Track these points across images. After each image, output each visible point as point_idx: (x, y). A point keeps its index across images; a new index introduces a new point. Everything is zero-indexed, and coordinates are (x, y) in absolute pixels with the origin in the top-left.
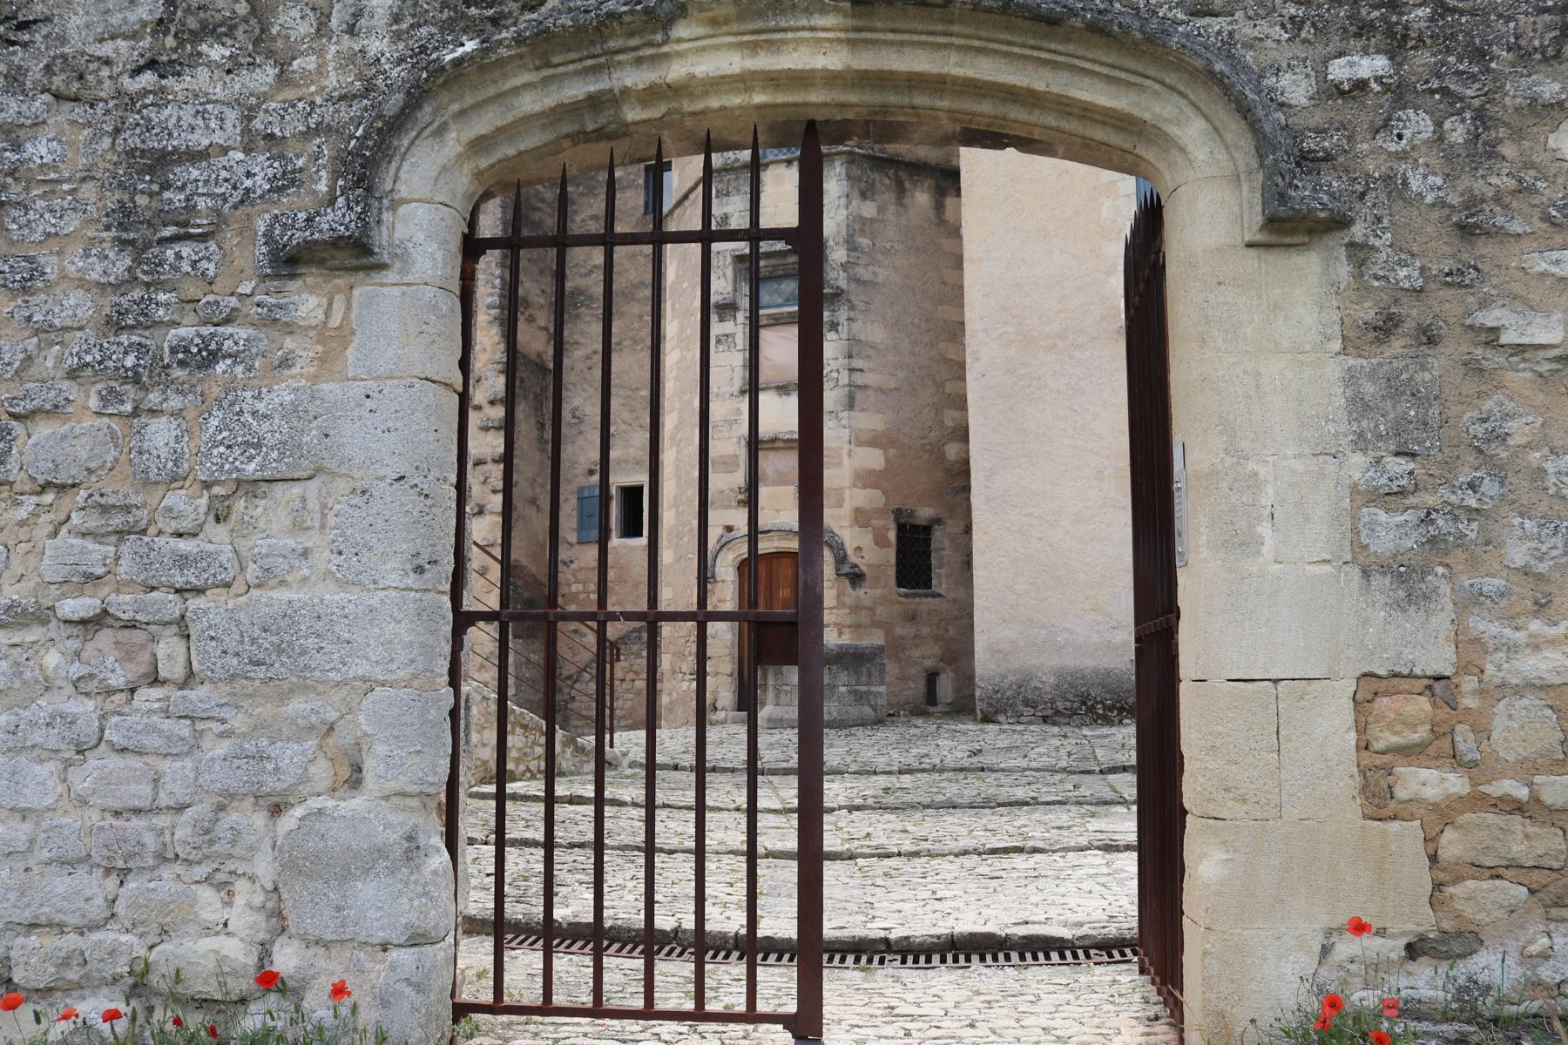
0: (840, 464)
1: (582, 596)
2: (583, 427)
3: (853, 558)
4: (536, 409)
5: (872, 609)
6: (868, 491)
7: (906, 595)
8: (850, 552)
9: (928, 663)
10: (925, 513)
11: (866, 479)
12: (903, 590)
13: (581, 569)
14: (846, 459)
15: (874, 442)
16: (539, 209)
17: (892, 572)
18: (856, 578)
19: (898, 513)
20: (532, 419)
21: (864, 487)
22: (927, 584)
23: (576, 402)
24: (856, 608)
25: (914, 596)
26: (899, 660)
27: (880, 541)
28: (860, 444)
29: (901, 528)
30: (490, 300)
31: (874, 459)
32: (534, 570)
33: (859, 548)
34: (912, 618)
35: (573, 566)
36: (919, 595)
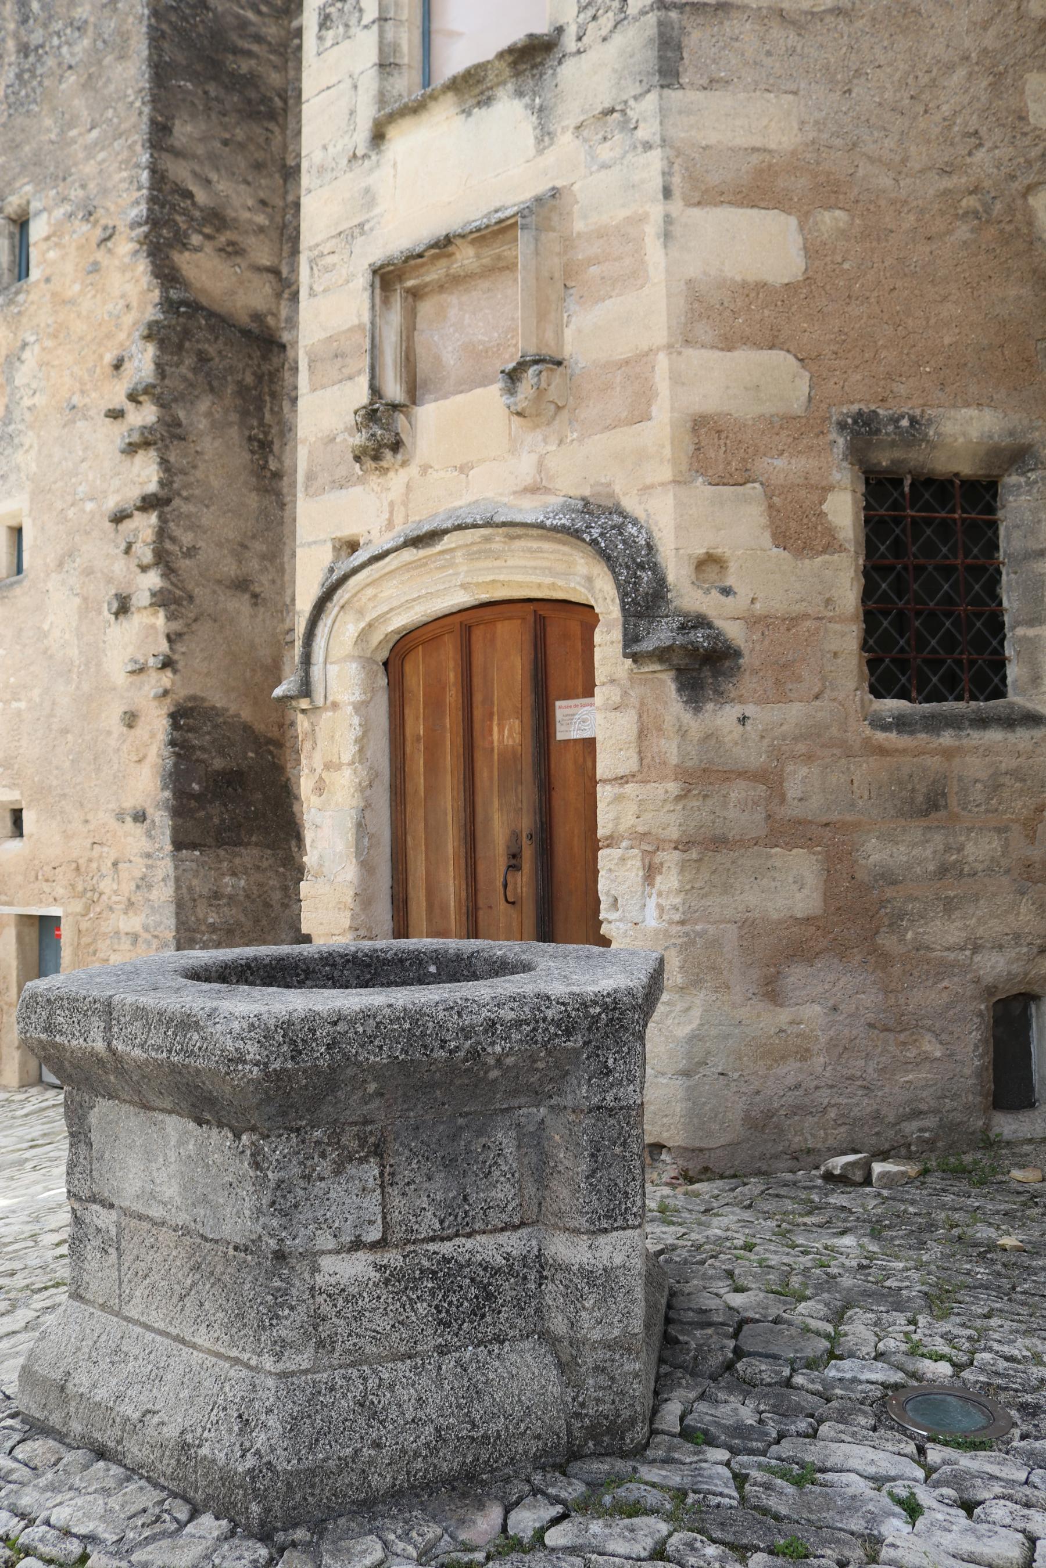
0: (636, 276)
3: (687, 595)
4: (245, 413)
5: (769, 779)
6: (745, 358)
7: (901, 724)
8: (676, 572)
9: (996, 966)
10: (963, 431)
11: (731, 315)
12: (892, 705)
14: (655, 254)
15: (759, 187)
16: (249, 54)
17: (846, 639)
18: (703, 665)
19: (862, 430)
20: (234, 432)
21: (728, 344)
22: (989, 681)
24: (701, 778)
25: (933, 724)
26: (883, 959)
27: (796, 529)
28: (707, 196)
29: (880, 489)
31: (766, 247)
32: (246, 714)
33: (709, 563)
34: (930, 803)
36: (955, 722)
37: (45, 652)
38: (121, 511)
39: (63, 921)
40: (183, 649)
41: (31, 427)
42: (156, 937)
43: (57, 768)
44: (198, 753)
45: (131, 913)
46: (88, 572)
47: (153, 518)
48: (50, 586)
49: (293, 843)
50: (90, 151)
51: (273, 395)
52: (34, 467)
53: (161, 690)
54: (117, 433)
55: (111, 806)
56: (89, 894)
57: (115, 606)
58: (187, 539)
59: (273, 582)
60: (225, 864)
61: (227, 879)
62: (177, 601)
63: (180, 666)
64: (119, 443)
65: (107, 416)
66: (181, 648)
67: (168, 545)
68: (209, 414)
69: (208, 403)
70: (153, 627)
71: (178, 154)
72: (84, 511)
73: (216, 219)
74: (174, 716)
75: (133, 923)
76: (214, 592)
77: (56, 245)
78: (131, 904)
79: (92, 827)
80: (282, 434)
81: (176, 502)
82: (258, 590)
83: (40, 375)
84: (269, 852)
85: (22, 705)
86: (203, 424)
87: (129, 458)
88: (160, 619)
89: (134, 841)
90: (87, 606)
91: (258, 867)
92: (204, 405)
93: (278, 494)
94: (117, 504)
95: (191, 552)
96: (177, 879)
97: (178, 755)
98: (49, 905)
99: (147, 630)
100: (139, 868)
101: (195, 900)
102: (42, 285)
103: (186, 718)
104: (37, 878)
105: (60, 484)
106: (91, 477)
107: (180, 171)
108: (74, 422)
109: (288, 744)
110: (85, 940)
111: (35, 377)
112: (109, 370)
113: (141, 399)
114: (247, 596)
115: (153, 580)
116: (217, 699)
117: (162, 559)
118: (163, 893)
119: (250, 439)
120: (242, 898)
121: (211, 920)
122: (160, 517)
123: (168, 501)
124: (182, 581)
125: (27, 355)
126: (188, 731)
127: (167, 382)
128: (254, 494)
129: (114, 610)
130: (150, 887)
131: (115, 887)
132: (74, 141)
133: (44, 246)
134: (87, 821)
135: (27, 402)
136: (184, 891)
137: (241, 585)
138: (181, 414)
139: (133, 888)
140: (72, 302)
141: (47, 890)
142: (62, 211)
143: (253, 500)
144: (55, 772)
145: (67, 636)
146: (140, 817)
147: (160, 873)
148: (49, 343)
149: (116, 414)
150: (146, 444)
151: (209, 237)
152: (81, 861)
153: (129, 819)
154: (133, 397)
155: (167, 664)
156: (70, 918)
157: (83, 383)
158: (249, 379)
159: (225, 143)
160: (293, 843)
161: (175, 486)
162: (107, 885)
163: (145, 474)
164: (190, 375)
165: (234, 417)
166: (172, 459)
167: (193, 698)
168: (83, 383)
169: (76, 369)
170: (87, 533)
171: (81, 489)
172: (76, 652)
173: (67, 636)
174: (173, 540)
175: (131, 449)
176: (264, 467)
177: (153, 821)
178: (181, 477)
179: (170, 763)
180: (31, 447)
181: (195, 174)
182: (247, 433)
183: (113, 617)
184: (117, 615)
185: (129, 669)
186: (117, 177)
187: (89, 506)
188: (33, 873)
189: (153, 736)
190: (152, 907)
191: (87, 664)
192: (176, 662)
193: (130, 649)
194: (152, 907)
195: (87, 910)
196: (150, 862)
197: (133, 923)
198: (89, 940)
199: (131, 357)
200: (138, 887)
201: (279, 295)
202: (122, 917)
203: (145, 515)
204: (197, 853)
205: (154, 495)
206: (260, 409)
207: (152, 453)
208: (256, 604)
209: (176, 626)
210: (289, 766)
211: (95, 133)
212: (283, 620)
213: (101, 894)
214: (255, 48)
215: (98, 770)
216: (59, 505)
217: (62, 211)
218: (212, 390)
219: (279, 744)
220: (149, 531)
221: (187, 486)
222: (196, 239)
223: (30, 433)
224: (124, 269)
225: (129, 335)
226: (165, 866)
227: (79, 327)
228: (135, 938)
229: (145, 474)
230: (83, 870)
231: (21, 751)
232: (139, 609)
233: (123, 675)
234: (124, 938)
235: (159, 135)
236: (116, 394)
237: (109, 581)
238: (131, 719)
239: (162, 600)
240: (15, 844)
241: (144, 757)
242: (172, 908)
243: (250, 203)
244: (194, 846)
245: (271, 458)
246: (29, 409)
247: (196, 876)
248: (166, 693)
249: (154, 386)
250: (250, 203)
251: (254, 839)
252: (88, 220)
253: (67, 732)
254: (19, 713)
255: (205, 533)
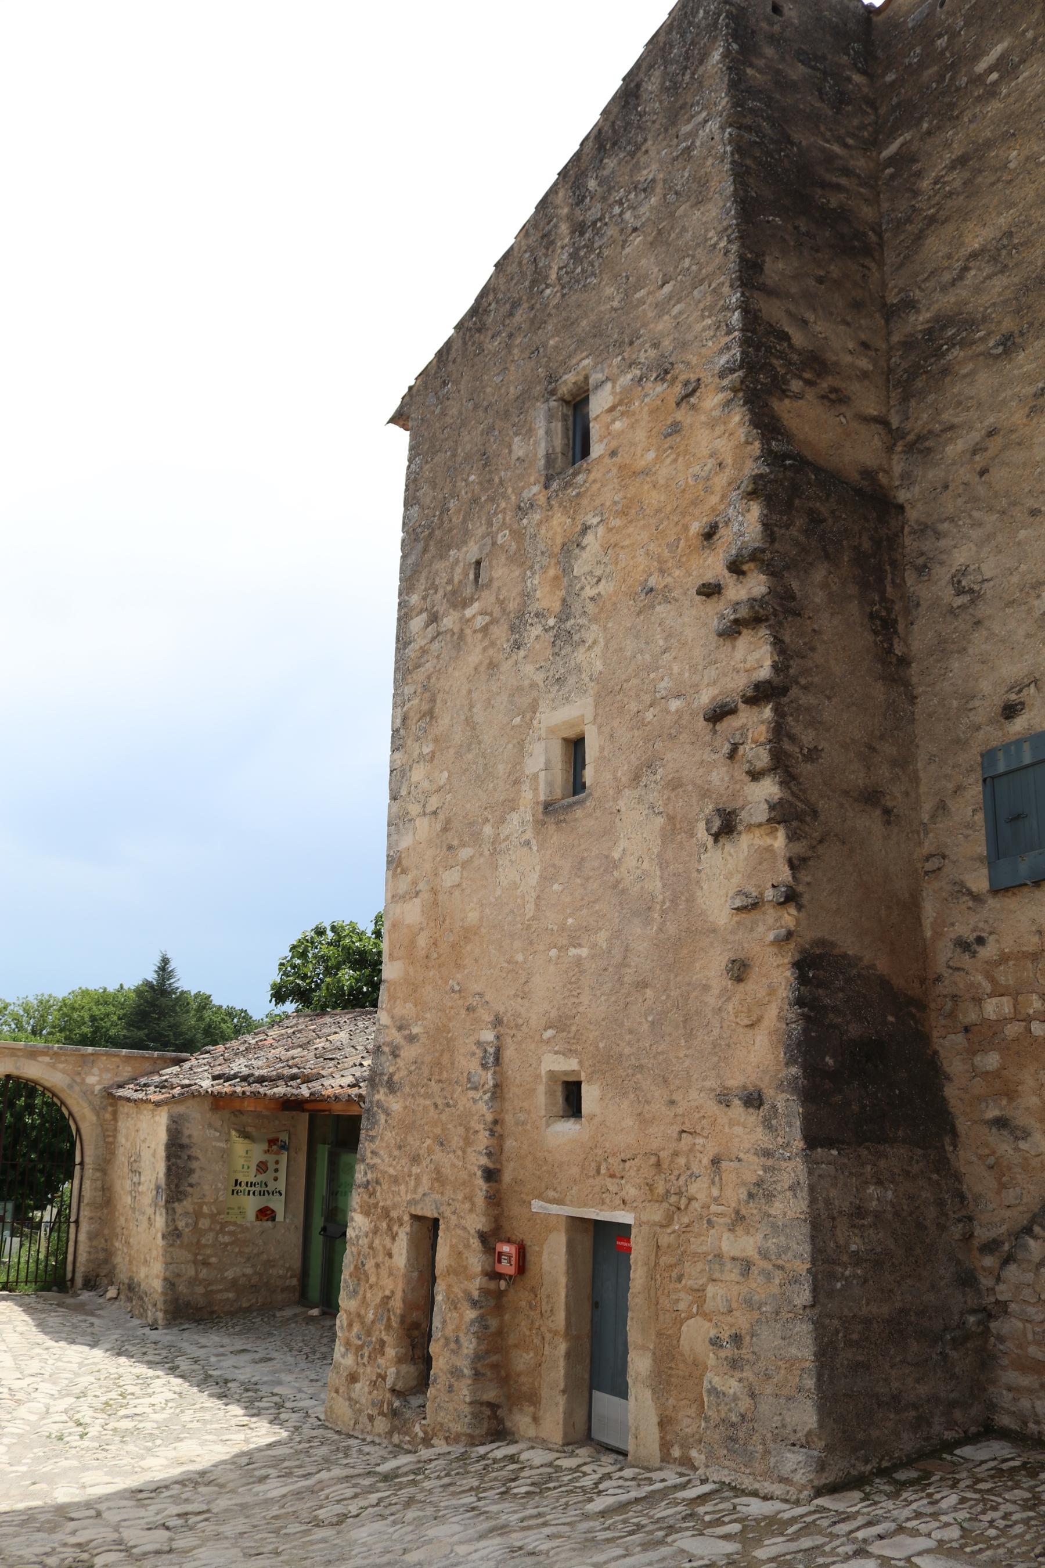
1: (1013, 1030)
2: (982, 610)
13: (1004, 958)
16: (838, 188)
20: (853, 607)
23: (960, 557)
30: (723, 360)
32: (883, 966)
35: (986, 952)
37: (615, 887)
38: (721, 706)
39: (634, 1231)
40: (808, 879)
41: (594, 619)
42: (780, 1268)
43: (631, 1032)
44: (831, 1015)
45: (739, 1230)
46: (675, 784)
47: (768, 712)
48: (621, 804)
49: (947, 1140)
50: (662, 308)
51: (893, 563)
52: (599, 666)
53: (783, 932)
54: (712, 615)
55: (708, 1084)
56: (673, 1199)
57: (717, 824)
58: (808, 737)
59: (907, 794)
60: (869, 1167)
61: (871, 1189)
62: (800, 817)
63: (805, 900)
64: (715, 624)
65: (699, 593)
66: (805, 877)
67: (787, 746)
68: (825, 585)
69: (824, 572)
70: (769, 849)
71: (771, 292)
72: (668, 712)
73: (816, 363)
74: (797, 965)
75: (746, 1244)
76: (841, 806)
77: (623, 414)
78: (739, 1218)
79: (680, 1111)
80: (907, 611)
81: (794, 691)
82: (890, 804)
83: (606, 560)
84: (920, 1152)
85: (584, 952)
86: (819, 597)
87: (728, 644)
88: (779, 841)
89: (745, 1132)
90: (675, 828)
91: (907, 1173)
92: (819, 574)
93: (907, 684)
94: (714, 698)
95: (812, 755)
96: (812, 1189)
97: (806, 1018)
98: (614, 1208)
99: (758, 855)
100: (753, 1169)
101: (834, 1219)
102: (607, 460)
103: (814, 967)
104: (598, 1172)
105: (634, 681)
106: (676, 669)
107: (774, 311)
108: (654, 607)
109: (933, 1006)
110: (664, 1260)
111: (599, 562)
112: (697, 542)
113: (745, 567)
114: (878, 812)
115: (769, 789)
116: (849, 945)
117: (781, 764)
118: (790, 1207)
119: (872, 616)
120: (890, 1216)
121: (854, 1247)
122: (776, 710)
123: (784, 691)
124: (804, 791)
125: (589, 539)
126: (818, 986)
127: (777, 545)
128: (879, 684)
129: (715, 829)
130: (770, 1197)
131: (715, 1192)
132: (642, 302)
133: (608, 418)
134: (672, 1102)
135: (589, 592)
136: (821, 1205)
137: (871, 797)
138: (795, 585)
139: (744, 1196)
140: (646, 472)
141: (613, 1188)
142: (629, 376)
143: (879, 691)
144: (628, 1037)
145: (646, 865)
146: (753, 1100)
147: (786, 1179)
148: (617, 522)
149: (710, 591)
150: (754, 621)
151: (809, 383)
152: (662, 1154)
153: (737, 1102)
154: (736, 568)
155: (791, 897)
156: (645, 1229)
157: (661, 561)
158: (867, 545)
159: (820, 280)
160: (947, 1140)
161: (792, 671)
162: (699, 1189)
163: (755, 657)
164: (802, 538)
165: (852, 590)
166: (787, 639)
167: (821, 942)
168: (661, 561)
169: (652, 546)
170: (672, 738)
171: (662, 685)
172: (659, 884)
173: (646, 865)
174: (792, 738)
175: (732, 631)
176: (890, 651)
177: (774, 1107)
178: (798, 661)
179: (797, 1028)
180: (595, 642)
181: (789, 313)
182: (868, 609)
183: (711, 839)
184: (716, 837)
185: (738, 903)
186: (699, 327)
187: (675, 705)
188: (593, 1165)
189: (772, 992)
190: (774, 1226)
191: (674, 901)
192: (801, 895)
193: (736, 879)
194: (774, 1226)
195: (669, 1220)
196: (770, 1162)
197: (746, 1244)
198: (672, 1260)
199: (727, 523)
200: (751, 1195)
201: (890, 449)
202: (726, 1235)
203: (755, 709)
204: (835, 1152)
205: (768, 682)
206: (881, 580)
207: (764, 631)
208: (888, 823)
209: (800, 848)
210: (935, 1034)
211: (667, 288)
212: (920, 844)
213: (690, 1200)
214: (843, 181)
215: (690, 1036)
216: (634, 707)
217: (629, 376)
218: (827, 557)
219: (922, 1006)
220: (763, 728)
221: (805, 672)
222: (796, 385)
223: (594, 627)
224: (712, 425)
225: (723, 497)
226: (793, 1170)
227: (655, 498)
228: (746, 1266)
229: (755, 657)
230: (665, 1166)
231: (581, 1009)
232: (750, 827)
233: (727, 910)
234: (729, 1265)
235: (750, 274)
236: (713, 566)
237: (705, 794)
238: (739, 970)
239: (782, 815)
240: (568, 1128)
241: (759, 1020)
242: (806, 1229)
243: (851, 345)
244: (829, 1143)
245: (896, 641)
246: (592, 599)
247: (834, 1185)
248: (790, 935)
249: (763, 551)
250: (851, 345)
251: (900, 1133)
252: (663, 380)
253: (646, 986)
254: (578, 961)
255: (828, 730)
